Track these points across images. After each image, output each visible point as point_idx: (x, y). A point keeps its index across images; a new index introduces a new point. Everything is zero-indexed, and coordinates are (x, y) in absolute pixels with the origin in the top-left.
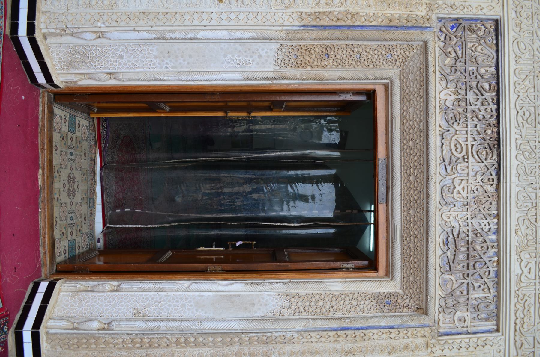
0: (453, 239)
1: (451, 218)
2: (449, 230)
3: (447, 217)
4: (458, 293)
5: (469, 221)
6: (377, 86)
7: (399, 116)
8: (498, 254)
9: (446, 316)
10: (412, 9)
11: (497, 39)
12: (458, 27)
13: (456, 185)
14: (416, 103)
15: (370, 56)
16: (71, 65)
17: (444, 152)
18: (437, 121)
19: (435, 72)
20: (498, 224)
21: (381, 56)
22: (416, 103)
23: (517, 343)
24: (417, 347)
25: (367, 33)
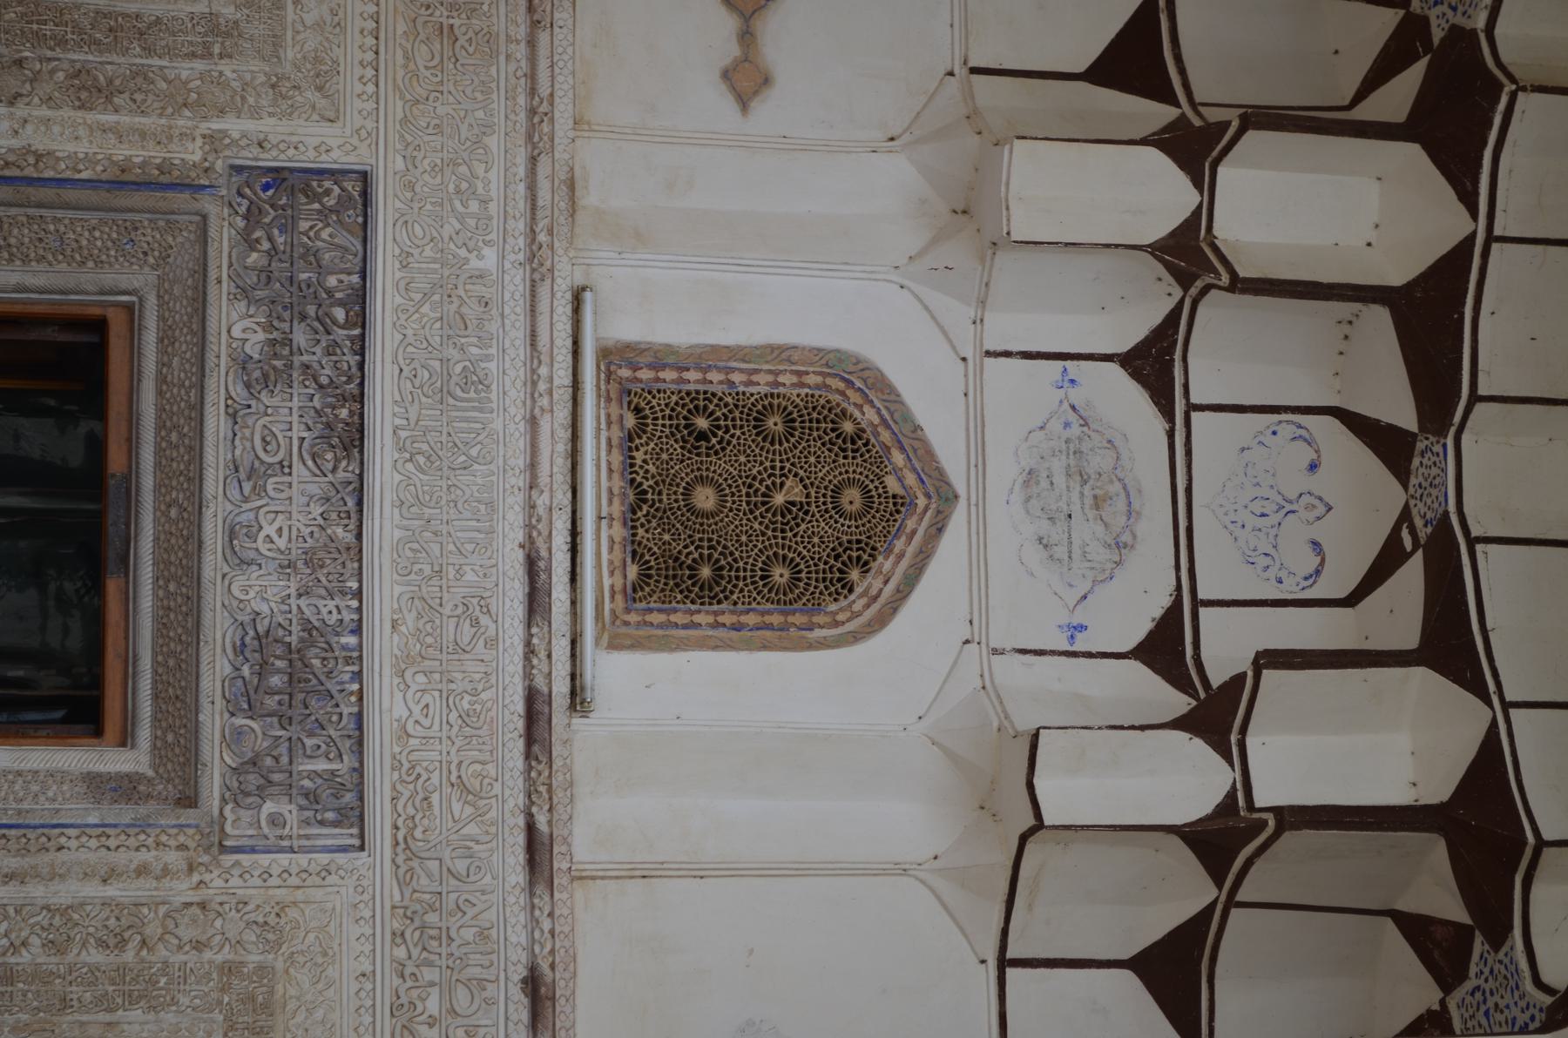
1: (252, 594)
2: (247, 619)
3: (245, 591)
4: (269, 761)
5: (292, 601)
6: (111, 309)
7: (152, 376)
8: (358, 676)
9: (242, 812)
10: (173, 147)
11: (365, 216)
12: (281, 188)
13: (264, 524)
14: (184, 347)
15: (84, 243)
17: (238, 452)
18: (221, 385)
19: (220, 282)
20: (359, 610)
21: (109, 244)
22: (184, 347)
23: (401, 871)
24: (166, 871)
25: (71, 195)
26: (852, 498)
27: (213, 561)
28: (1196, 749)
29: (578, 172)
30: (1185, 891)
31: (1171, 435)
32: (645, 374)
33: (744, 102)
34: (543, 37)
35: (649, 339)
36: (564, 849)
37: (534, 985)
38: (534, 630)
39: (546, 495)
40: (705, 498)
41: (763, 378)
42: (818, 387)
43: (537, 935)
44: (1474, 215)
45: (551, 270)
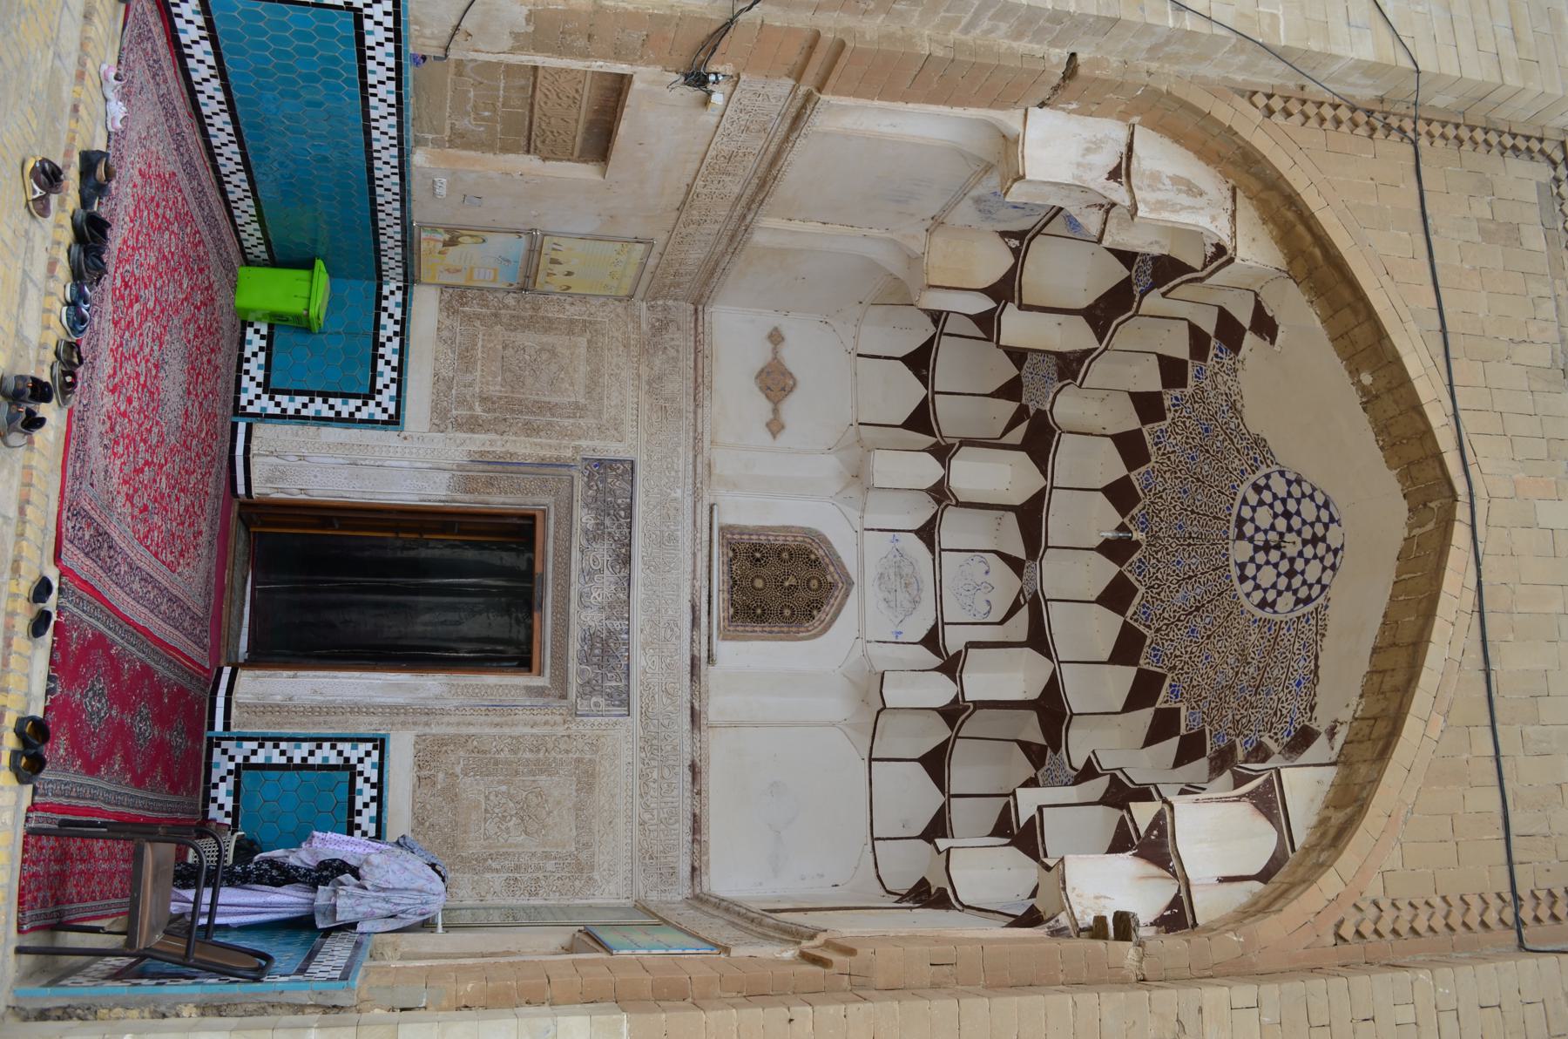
0: (590, 638)
3: (585, 618)
12: (601, 466)
16: (268, 480)
18: (578, 540)
25: (522, 468)
27: (574, 606)
28: (943, 678)
30: (941, 733)
33: (774, 435)
37: (694, 769)
40: (759, 583)
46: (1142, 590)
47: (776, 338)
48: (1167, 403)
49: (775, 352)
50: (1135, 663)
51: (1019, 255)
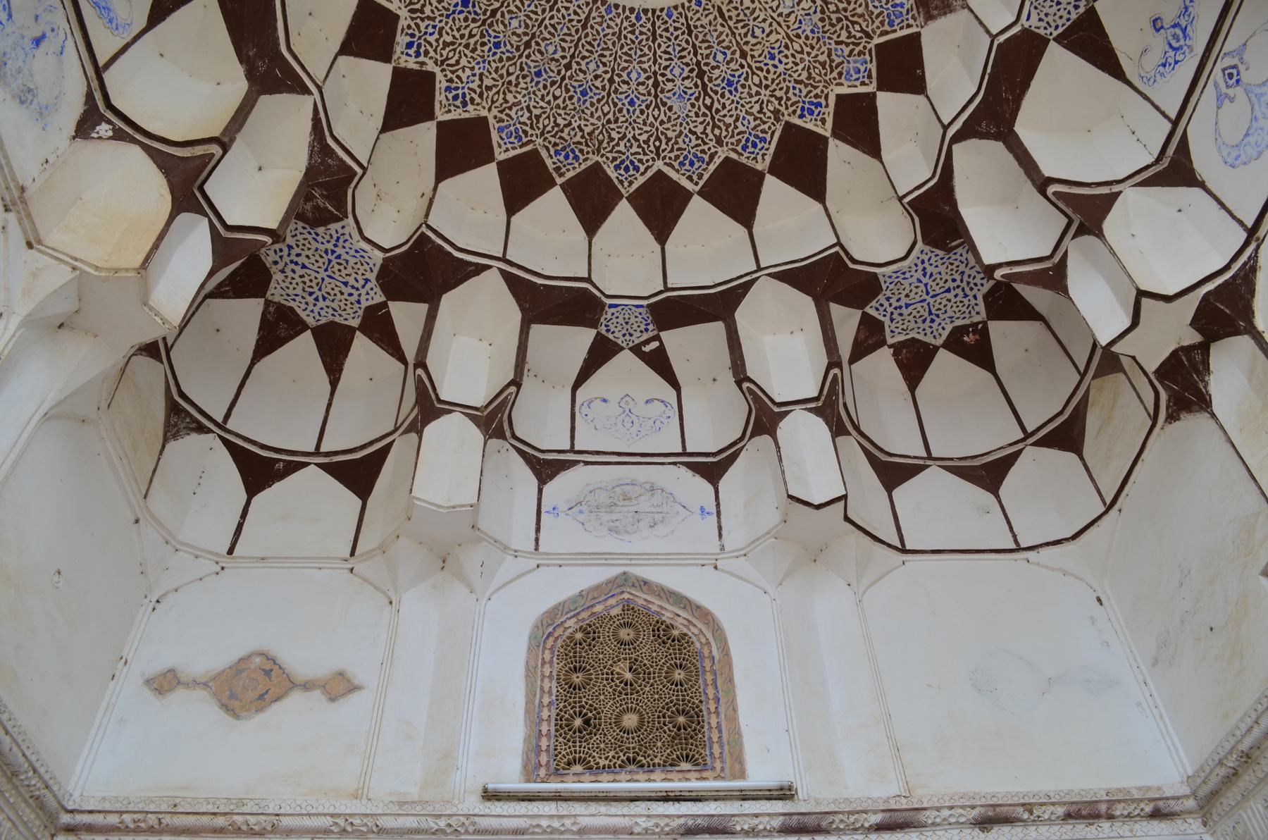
26: (625, 634)
28: (784, 429)
29: (394, 799)
31: (587, 463)
32: (544, 758)
33: (354, 688)
34: (286, 822)
35: (520, 752)
36: (892, 802)
37: (985, 823)
38: (738, 828)
39: (639, 820)
40: (630, 720)
41: (547, 684)
42: (552, 653)
43: (953, 820)
44: (489, 267)
45: (468, 816)
46: (659, 165)
47: (165, 683)
48: (411, 64)
49: (195, 684)
50: (760, 176)
51: (129, 131)
